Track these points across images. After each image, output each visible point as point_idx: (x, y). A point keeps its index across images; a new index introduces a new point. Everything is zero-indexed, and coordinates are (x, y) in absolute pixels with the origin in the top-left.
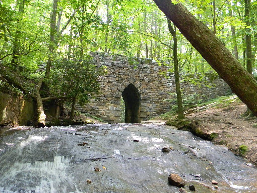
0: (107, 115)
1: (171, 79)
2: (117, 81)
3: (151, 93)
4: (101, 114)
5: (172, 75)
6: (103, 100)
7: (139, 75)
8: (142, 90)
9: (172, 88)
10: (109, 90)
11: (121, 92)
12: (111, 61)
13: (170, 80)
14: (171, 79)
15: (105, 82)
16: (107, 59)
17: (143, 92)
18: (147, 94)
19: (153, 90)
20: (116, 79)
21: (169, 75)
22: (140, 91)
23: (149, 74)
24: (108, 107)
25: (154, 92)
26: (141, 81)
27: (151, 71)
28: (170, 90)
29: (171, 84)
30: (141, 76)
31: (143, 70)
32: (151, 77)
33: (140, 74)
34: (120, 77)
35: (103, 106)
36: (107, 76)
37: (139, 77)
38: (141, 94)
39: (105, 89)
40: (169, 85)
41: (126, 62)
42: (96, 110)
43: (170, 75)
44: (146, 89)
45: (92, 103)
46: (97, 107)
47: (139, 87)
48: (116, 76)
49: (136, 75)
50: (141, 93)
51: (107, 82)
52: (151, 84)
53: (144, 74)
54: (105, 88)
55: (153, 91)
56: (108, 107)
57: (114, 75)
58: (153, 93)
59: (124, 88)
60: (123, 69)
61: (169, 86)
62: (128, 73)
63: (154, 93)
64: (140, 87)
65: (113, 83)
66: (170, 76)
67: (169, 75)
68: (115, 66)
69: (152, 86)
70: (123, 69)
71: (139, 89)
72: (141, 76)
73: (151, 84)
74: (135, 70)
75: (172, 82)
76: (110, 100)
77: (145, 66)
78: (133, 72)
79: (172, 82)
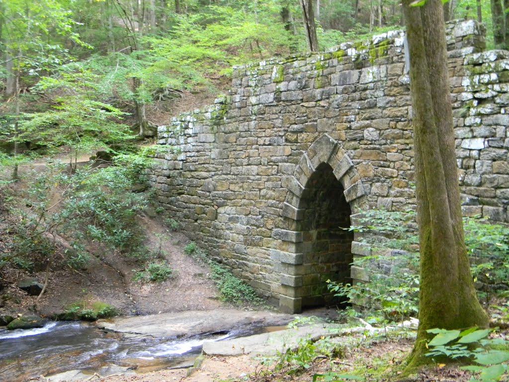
0: (264, 278)
1: (479, 115)
2: (288, 156)
3: (389, 199)
4: (252, 273)
5: (490, 94)
6: (258, 227)
7: (350, 122)
8: (354, 188)
9: (484, 168)
10: (271, 192)
11: (297, 197)
12: (274, 87)
13: (478, 120)
14: (479, 115)
15: (261, 164)
16: (266, 84)
17: (359, 194)
18: (377, 201)
19: (398, 186)
20: (284, 150)
21: (470, 96)
22: (349, 191)
23: (384, 108)
24: (267, 252)
25: (402, 194)
26: (355, 149)
27: (392, 93)
28: (476, 179)
29: (479, 144)
30: (354, 125)
31: (363, 93)
32: (392, 123)
33: (352, 117)
34: (296, 141)
35: (255, 245)
36: (264, 145)
37: (350, 128)
38: (353, 201)
39: (260, 190)
40: (467, 153)
41: (310, 78)
42: (243, 259)
43: (478, 95)
44: (372, 181)
45: (235, 234)
46: (244, 246)
47: (347, 173)
48: (286, 140)
49: (338, 126)
50: (355, 200)
51: (264, 165)
52: (389, 156)
53: (367, 115)
54: (259, 184)
55: (397, 189)
56: (267, 252)
57: (282, 136)
58: (395, 199)
59: (304, 180)
60: (303, 110)
61: (469, 157)
62: (316, 121)
63: (401, 199)
64: (351, 174)
65: (278, 165)
66: (475, 103)
67: (470, 96)
68: (284, 101)
69: (392, 165)
70: (303, 110)
71: (347, 185)
72: (354, 125)
73: (389, 156)
74: (335, 104)
75: (487, 133)
76: (270, 227)
77: (370, 74)
78: (331, 114)
79: (483, 130)
